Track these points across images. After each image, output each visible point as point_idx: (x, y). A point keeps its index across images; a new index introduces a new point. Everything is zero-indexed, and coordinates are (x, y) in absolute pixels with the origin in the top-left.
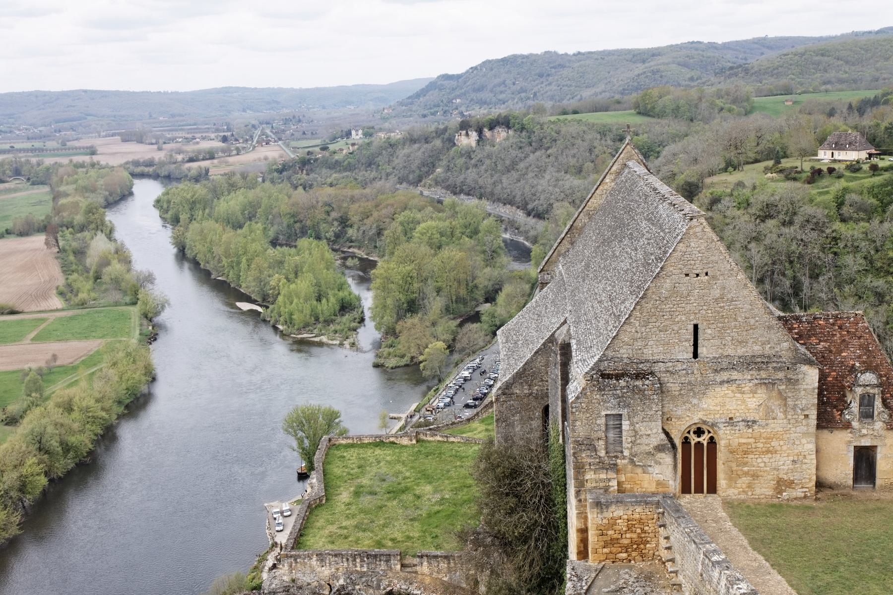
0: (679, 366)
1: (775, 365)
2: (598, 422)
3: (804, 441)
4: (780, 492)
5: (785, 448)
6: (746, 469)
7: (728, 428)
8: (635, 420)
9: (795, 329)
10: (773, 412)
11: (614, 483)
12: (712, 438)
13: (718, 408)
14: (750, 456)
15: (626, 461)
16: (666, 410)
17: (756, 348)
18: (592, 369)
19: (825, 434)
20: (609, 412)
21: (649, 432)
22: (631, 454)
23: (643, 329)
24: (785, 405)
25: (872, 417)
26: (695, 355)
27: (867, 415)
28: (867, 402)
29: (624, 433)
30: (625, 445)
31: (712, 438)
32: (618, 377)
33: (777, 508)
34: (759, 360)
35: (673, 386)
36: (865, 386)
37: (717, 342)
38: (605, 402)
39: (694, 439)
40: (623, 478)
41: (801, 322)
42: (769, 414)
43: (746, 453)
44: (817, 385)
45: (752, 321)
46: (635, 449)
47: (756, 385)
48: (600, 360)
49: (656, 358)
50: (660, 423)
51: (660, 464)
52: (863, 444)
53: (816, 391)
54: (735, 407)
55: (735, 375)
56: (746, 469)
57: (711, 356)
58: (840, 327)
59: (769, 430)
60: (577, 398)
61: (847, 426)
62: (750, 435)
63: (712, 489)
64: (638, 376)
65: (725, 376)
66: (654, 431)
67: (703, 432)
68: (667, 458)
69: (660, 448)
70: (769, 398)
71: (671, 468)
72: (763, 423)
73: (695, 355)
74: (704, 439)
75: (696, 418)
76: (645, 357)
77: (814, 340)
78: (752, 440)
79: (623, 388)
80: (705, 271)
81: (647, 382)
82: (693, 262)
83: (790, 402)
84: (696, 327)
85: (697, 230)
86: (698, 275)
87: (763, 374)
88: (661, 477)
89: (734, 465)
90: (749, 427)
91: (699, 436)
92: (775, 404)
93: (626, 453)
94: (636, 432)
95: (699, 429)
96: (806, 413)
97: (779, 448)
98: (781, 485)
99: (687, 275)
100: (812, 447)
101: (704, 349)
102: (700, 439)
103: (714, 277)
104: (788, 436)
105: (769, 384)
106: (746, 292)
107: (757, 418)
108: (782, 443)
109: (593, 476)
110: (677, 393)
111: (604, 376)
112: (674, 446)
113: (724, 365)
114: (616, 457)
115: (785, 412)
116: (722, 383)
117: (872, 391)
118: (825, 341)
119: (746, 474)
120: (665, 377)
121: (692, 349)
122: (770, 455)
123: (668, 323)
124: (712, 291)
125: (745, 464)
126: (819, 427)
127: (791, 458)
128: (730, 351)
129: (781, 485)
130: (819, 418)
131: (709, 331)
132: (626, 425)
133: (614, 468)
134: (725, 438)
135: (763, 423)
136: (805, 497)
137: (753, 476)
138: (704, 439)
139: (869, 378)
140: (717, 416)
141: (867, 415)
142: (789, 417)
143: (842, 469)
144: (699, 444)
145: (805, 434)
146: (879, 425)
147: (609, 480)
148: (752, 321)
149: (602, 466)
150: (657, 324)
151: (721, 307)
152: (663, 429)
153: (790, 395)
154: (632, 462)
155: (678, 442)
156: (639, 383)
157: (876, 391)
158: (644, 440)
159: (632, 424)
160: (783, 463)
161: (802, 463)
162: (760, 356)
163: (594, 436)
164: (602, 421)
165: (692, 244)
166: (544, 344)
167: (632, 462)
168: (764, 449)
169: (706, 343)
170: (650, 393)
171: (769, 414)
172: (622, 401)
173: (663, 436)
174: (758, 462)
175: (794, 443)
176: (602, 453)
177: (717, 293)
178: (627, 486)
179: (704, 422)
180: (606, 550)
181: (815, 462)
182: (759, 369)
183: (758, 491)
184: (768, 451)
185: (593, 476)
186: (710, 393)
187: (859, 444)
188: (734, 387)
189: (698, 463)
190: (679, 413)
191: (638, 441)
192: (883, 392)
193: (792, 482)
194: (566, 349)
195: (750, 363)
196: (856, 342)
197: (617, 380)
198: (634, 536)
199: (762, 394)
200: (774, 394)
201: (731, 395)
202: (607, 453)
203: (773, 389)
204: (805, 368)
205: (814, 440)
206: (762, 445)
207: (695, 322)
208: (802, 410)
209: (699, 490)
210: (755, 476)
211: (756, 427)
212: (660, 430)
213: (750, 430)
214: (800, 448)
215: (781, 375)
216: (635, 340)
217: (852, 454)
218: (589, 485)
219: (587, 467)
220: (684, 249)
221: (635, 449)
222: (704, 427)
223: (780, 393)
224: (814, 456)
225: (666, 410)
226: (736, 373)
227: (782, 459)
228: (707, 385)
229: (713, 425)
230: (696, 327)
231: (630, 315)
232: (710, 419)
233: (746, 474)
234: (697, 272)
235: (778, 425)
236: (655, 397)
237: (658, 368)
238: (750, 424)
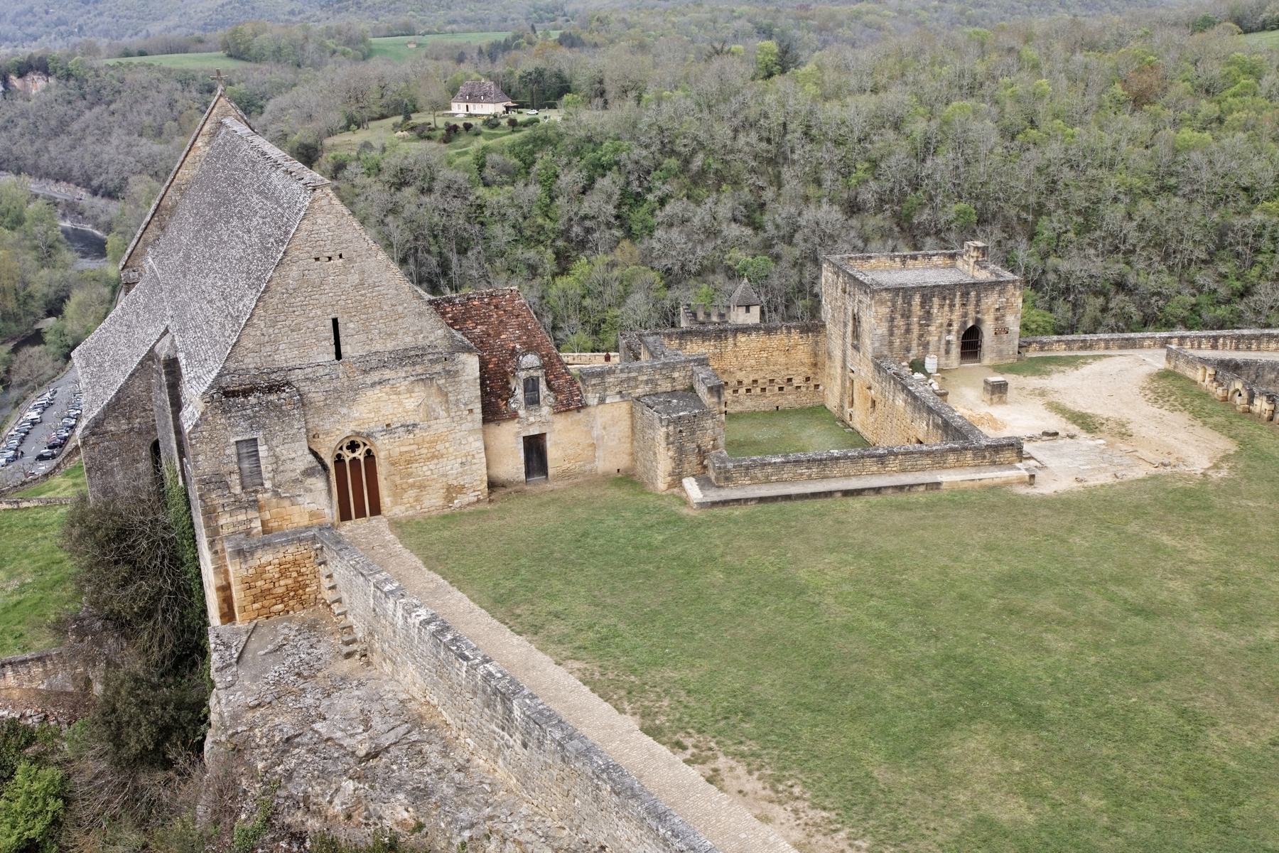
0: (321, 371)
1: (430, 357)
2: (227, 452)
3: (471, 439)
4: (451, 501)
5: (451, 450)
6: (411, 481)
8: (274, 443)
11: (257, 525)
12: (369, 451)
13: (372, 415)
16: (310, 426)
17: (408, 339)
18: (211, 387)
19: (492, 427)
20: (239, 438)
21: (293, 455)
22: (274, 485)
23: (271, 331)
24: (447, 401)
25: (538, 402)
26: (339, 355)
27: (533, 401)
28: (531, 386)
29: (263, 462)
30: (265, 475)
31: (369, 451)
32: (246, 393)
33: (449, 519)
34: (412, 353)
35: (316, 395)
37: (362, 337)
38: (233, 426)
39: (348, 456)
40: (267, 516)
41: (454, 304)
42: (430, 415)
43: (409, 462)
44: (478, 374)
45: (400, 309)
46: (278, 478)
47: (412, 382)
48: (220, 375)
49: (291, 364)
50: (305, 443)
51: (311, 491)
52: (532, 434)
55: (387, 374)
56: (411, 481)
58: (496, 307)
60: (196, 426)
61: (514, 416)
63: (376, 510)
64: (272, 388)
65: (375, 376)
66: (300, 453)
67: (358, 446)
68: (318, 483)
69: (308, 473)
70: (429, 396)
71: (324, 493)
72: (425, 425)
73: (339, 355)
74: (360, 454)
75: (347, 430)
76: (277, 365)
77: (470, 324)
78: (415, 447)
79: (253, 406)
81: (283, 395)
83: (452, 398)
84: (335, 321)
85: (324, 202)
86: (330, 259)
87: (419, 369)
88: (314, 507)
89: (397, 480)
90: (409, 432)
91: (353, 452)
92: (435, 401)
93: (268, 485)
94: (277, 458)
95: (353, 442)
97: (444, 451)
98: (452, 491)
99: (317, 259)
100: (480, 444)
102: (355, 455)
103: (350, 260)
105: (426, 380)
106: (389, 275)
107: (417, 421)
108: (447, 445)
109: (229, 520)
111: (227, 394)
112: (325, 468)
113: (374, 364)
114: (256, 492)
115: (447, 410)
116: (373, 385)
117: (535, 374)
119: (412, 486)
120: (305, 387)
123: (300, 320)
124: (350, 277)
125: (410, 475)
126: (485, 421)
127: (459, 461)
128: (378, 347)
129: (452, 491)
130: (484, 412)
131: (351, 325)
132: (263, 450)
133: (256, 505)
134: (384, 448)
135: (425, 425)
136: (479, 501)
137: (419, 487)
138: (360, 454)
139: (531, 360)
141: (533, 401)
143: (513, 465)
144: (355, 461)
146: (545, 410)
147: (251, 521)
148: (400, 309)
149: (239, 505)
152: (310, 449)
154: (276, 494)
155: (329, 461)
156: (273, 397)
157: (540, 373)
158: (289, 466)
159: (270, 449)
160: (451, 467)
161: (471, 464)
162: (413, 349)
163: (224, 469)
164: (232, 450)
165: (319, 221)
166: (141, 363)
167: (276, 494)
169: (349, 340)
171: (430, 415)
172: (254, 422)
173: (311, 457)
174: (424, 470)
176: (237, 490)
177: (355, 278)
178: (274, 524)
179: (358, 434)
180: (256, 606)
181: (484, 460)
182: (414, 364)
183: (427, 503)
184: (434, 457)
185: (229, 520)
186: (362, 398)
188: (387, 389)
189: (355, 481)
190: (327, 427)
192: (546, 374)
193: (463, 487)
194: (172, 366)
195: (403, 358)
196: (514, 321)
197: (246, 397)
198: (290, 581)
199: (420, 392)
200: (434, 390)
201: (385, 397)
202: (243, 488)
204: (464, 357)
205: (481, 436)
207: (333, 316)
208: (466, 404)
209: (361, 513)
210: (422, 487)
211: (417, 431)
212: (307, 451)
214: (467, 448)
215: (438, 368)
217: (522, 446)
218: (225, 532)
219: (220, 509)
220: (309, 228)
221: (278, 478)
222: (359, 440)
223: (439, 388)
224: (483, 455)
225: (310, 426)
226: (388, 371)
228: (356, 390)
229: (369, 436)
230: (335, 321)
231: (252, 315)
232: (364, 429)
233: (412, 486)
234: (329, 254)
235: (441, 425)
237: (295, 376)
238: (410, 428)
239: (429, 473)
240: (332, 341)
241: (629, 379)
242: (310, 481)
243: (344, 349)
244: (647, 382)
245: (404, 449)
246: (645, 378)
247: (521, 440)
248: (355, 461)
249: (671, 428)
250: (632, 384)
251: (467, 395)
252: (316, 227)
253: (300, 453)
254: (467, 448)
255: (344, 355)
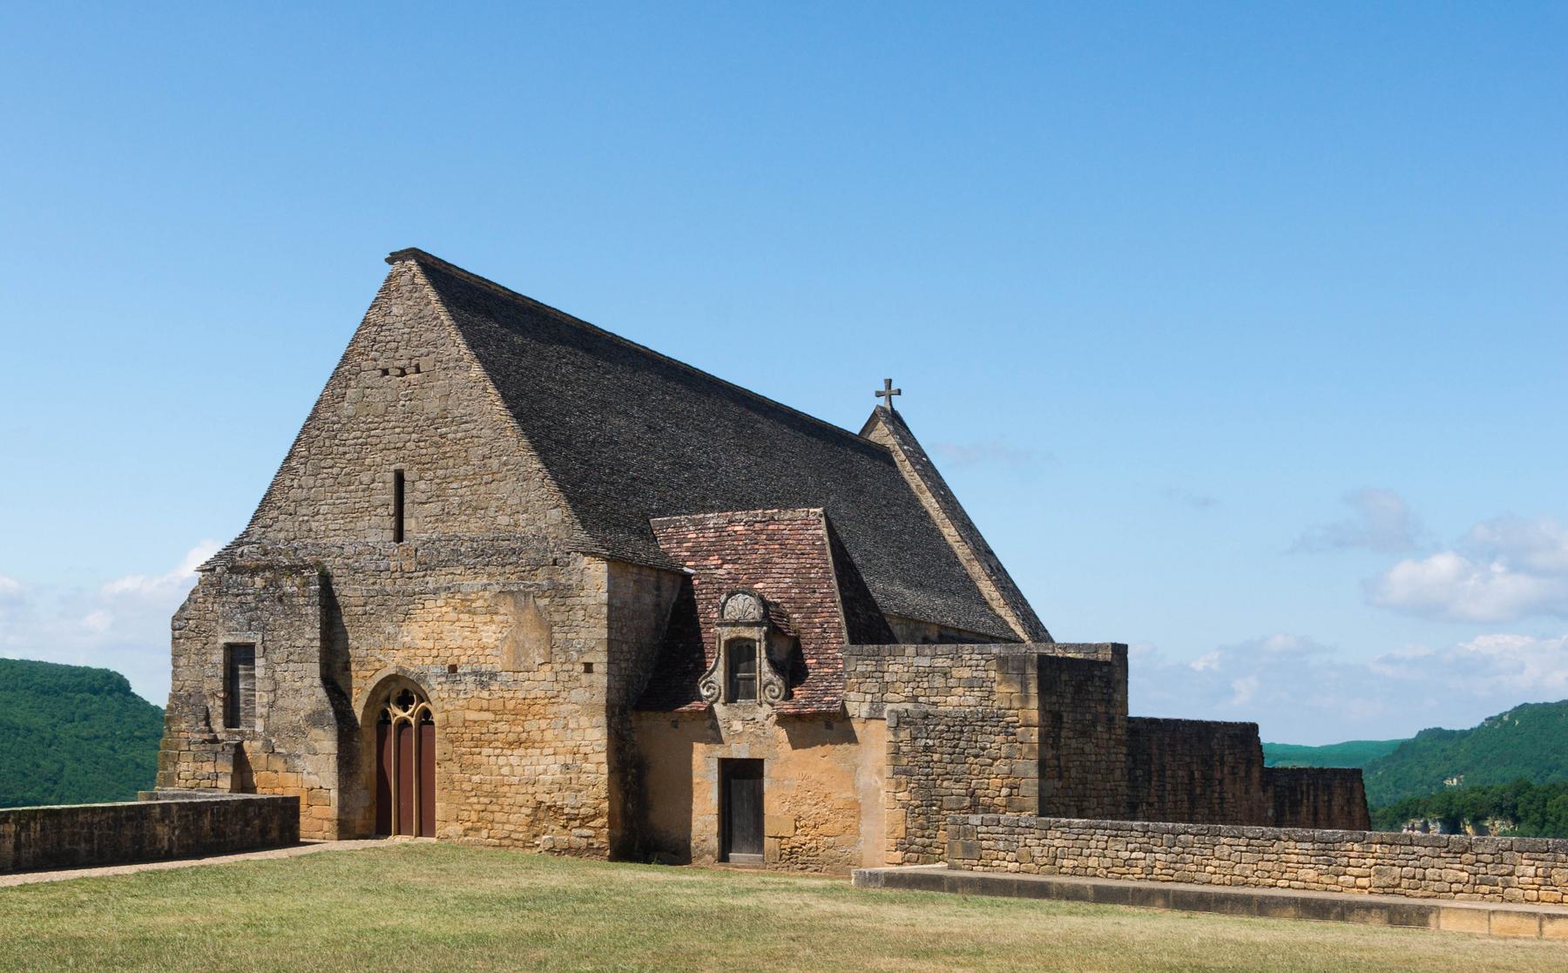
3: (584, 721)
5: (549, 735)
6: (476, 779)
7: (446, 687)
9: (689, 540)
10: (527, 655)
13: (430, 644)
14: (486, 751)
15: (258, 744)
18: (219, 556)
20: (231, 640)
22: (266, 728)
26: (399, 536)
30: (259, 710)
32: (254, 572)
36: (735, 624)
38: (226, 617)
43: (478, 743)
48: (239, 542)
52: (735, 755)
53: (605, 610)
54: (459, 643)
56: (476, 779)
57: (425, 537)
59: (520, 695)
62: (485, 704)
69: (315, 719)
71: (333, 763)
73: (399, 536)
77: (714, 560)
80: (414, 362)
82: (393, 345)
84: (400, 477)
86: (403, 373)
90: (483, 685)
92: (531, 636)
93: (259, 726)
94: (276, 683)
96: (587, 659)
97: (536, 735)
101: (413, 521)
104: (555, 708)
105: (520, 596)
108: (543, 724)
110: (360, 610)
116: (435, 592)
117: (747, 633)
118: (734, 562)
121: (390, 523)
122: (521, 751)
127: (561, 759)
128: (456, 528)
131: (421, 485)
140: (428, 661)
142: (557, 667)
145: (588, 708)
148: (494, 463)
150: (335, 471)
151: (441, 436)
153: (557, 617)
157: (755, 633)
159: (269, 667)
160: (545, 767)
164: (218, 657)
165: (395, 310)
168: (512, 737)
170: (301, 601)
173: (321, 693)
175: (565, 727)
177: (433, 406)
186: (418, 613)
187: (726, 756)
191: (280, 703)
195: (492, 553)
196: (791, 563)
200: (529, 615)
201: (453, 616)
203: (526, 606)
206: (506, 728)
207: (398, 466)
211: (495, 687)
212: (318, 681)
213: (485, 694)
216: (298, 503)
220: (380, 321)
227: (544, 761)
230: (400, 477)
232: (413, 669)
236: (309, 610)
238: (484, 679)
239: (505, 770)
240: (392, 509)
241: (932, 671)
242: (316, 733)
243: (409, 524)
244: (970, 685)
245: (472, 716)
246: (966, 673)
247: (715, 766)
248: (404, 723)
249: (904, 735)
250: (939, 682)
251: (583, 634)
252: (388, 320)
253: (307, 681)
254: (577, 736)
255: (406, 535)
